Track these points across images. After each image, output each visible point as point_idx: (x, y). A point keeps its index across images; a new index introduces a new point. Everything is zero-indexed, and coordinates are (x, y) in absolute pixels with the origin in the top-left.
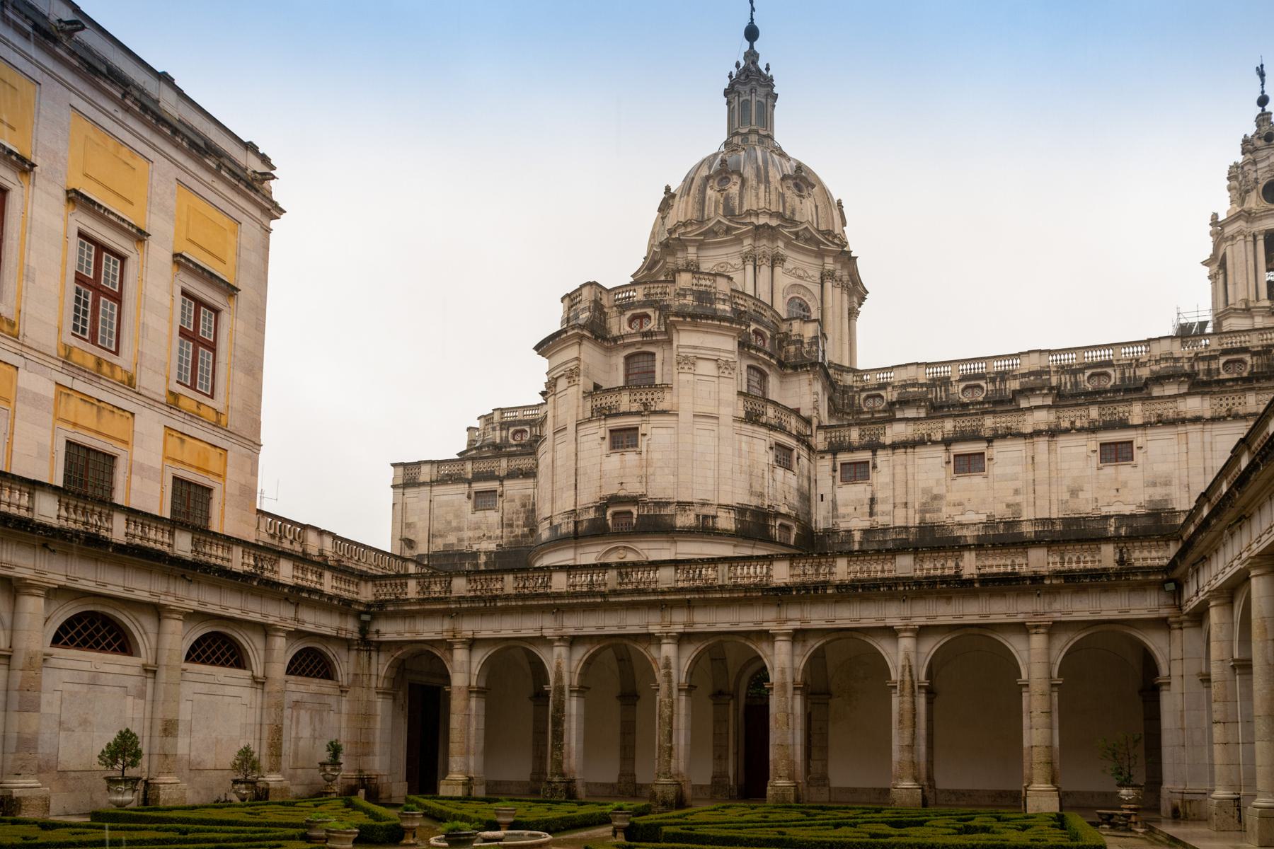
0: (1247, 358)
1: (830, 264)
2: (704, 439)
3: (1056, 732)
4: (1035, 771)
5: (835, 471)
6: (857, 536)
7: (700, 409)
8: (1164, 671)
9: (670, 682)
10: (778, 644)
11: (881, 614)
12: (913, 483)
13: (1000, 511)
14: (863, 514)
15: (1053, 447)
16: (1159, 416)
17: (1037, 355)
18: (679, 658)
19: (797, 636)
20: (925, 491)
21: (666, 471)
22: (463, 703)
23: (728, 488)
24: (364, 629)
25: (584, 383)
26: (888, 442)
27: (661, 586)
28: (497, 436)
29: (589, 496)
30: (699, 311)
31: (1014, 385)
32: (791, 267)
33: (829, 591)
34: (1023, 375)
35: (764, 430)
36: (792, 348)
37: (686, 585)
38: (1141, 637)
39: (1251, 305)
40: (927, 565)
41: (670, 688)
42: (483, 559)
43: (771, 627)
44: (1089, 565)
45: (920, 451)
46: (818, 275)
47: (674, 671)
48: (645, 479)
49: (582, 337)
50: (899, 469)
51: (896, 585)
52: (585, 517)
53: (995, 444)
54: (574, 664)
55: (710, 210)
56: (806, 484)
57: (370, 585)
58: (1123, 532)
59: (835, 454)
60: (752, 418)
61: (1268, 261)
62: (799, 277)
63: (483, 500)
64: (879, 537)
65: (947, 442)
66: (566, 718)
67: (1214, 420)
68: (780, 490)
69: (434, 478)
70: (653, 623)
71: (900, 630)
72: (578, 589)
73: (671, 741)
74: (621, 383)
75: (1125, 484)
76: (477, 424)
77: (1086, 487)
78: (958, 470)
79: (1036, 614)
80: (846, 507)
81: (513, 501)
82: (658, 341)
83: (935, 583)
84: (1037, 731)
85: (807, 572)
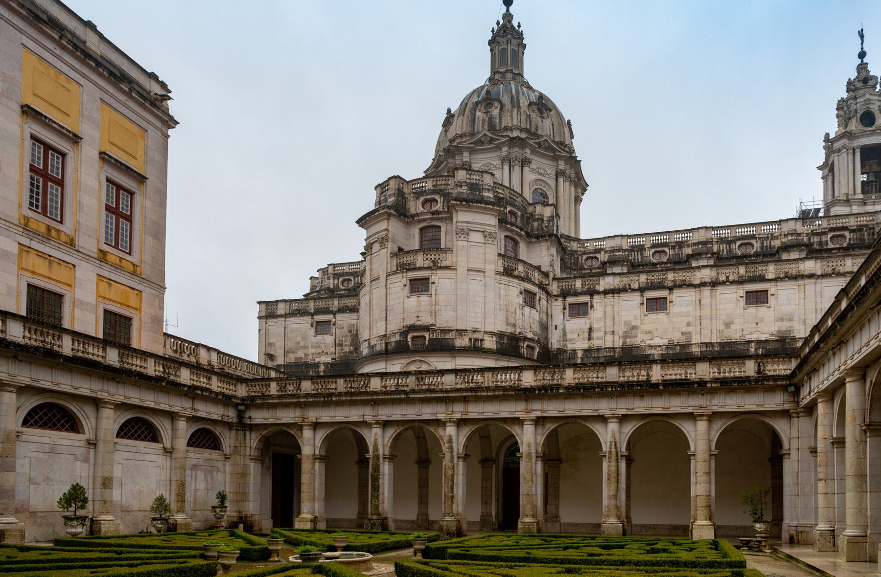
0: (847, 234)
1: (562, 165)
2: (475, 286)
3: (713, 486)
4: (698, 512)
5: (565, 309)
6: (580, 354)
7: (472, 266)
8: (786, 446)
9: (452, 452)
10: (525, 427)
11: (596, 407)
12: (617, 318)
13: (677, 337)
14: (584, 339)
15: (714, 294)
16: (787, 273)
17: (704, 230)
18: (458, 436)
19: (539, 421)
20: (627, 323)
21: (449, 308)
22: (310, 466)
23: (492, 320)
24: (240, 416)
25: (391, 247)
26: (601, 289)
27: (446, 387)
28: (331, 283)
29: (395, 325)
30: (471, 197)
31: (688, 251)
32: (535, 167)
33: (561, 391)
34: (694, 244)
35: (516, 281)
36: (536, 224)
37: (463, 386)
38: (771, 423)
39: (850, 197)
40: (628, 373)
41: (452, 456)
42: (322, 368)
43: (521, 415)
44: (737, 374)
45: (623, 296)
46: (554, 173)
47: (455, 445)
48: (434, 314)
49: (390, 215)
50: (609, 308)
51: (607, 387)
52: (393, 339)
53: (674, 291)
54: (386, 440)
55: (478, 126)
56: (545, 318)
57: (244, 385)
58: (760, 352)
59: (565, 297)
60: (508, 272)
61: (863, 166)
62: (541, 174)
63: (322, 328)
64: (595, 355)
65: (642, 290)
66: (381, 476)
67: (823, 276)
68: (528, 322)
69: (287, 312)
70: (440, 412)
71: (609, 418)
72: (388, 389)
73: (453, 492)
74: (417, 247)
75: (762, 320)
76: (317, 275)
77: (736, 321)
78: (649, 309)
79: (701, 407)
80: (572, 334)
81: (343, 328)
82: (443, 218)
83: (633, 386)
84: (701, 485)
85: (546, 378)
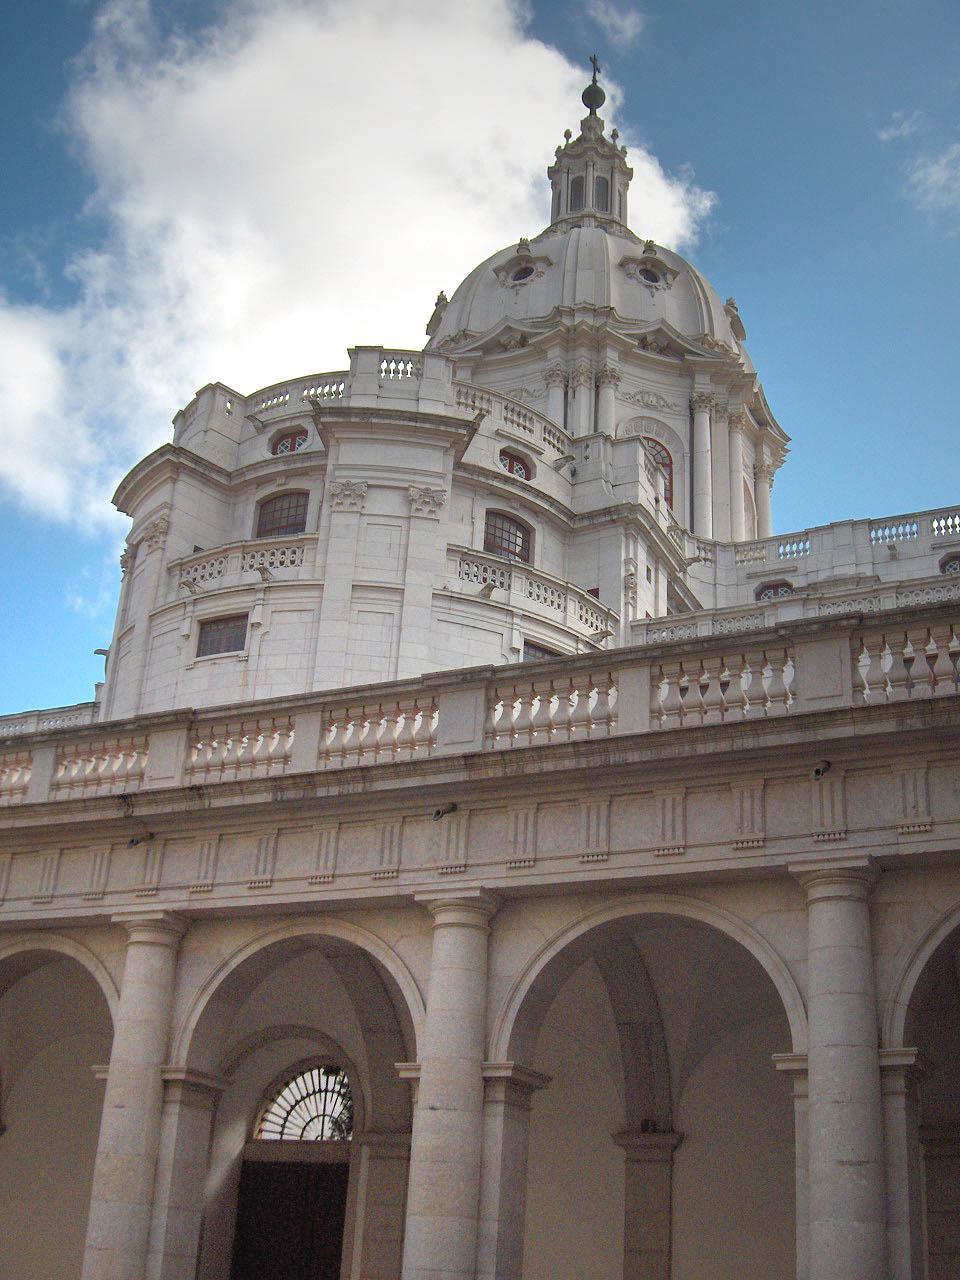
1: (703, 384)
32: (633, 390)
46: (684, 403)
49: (177, 468)
62: (647, 406)
